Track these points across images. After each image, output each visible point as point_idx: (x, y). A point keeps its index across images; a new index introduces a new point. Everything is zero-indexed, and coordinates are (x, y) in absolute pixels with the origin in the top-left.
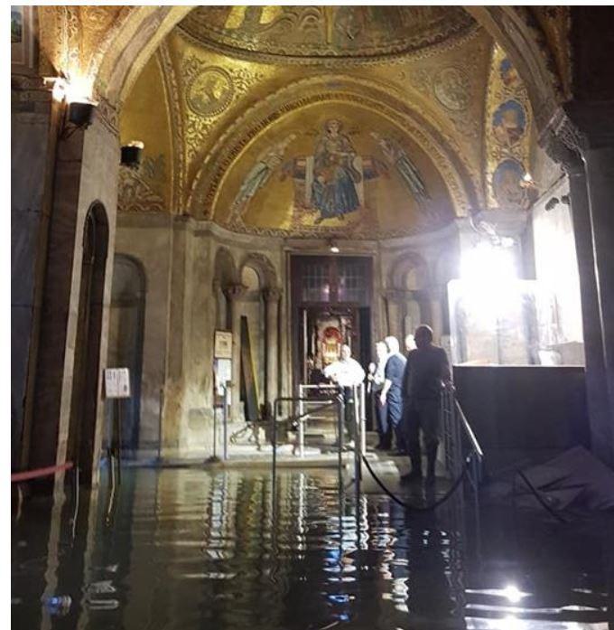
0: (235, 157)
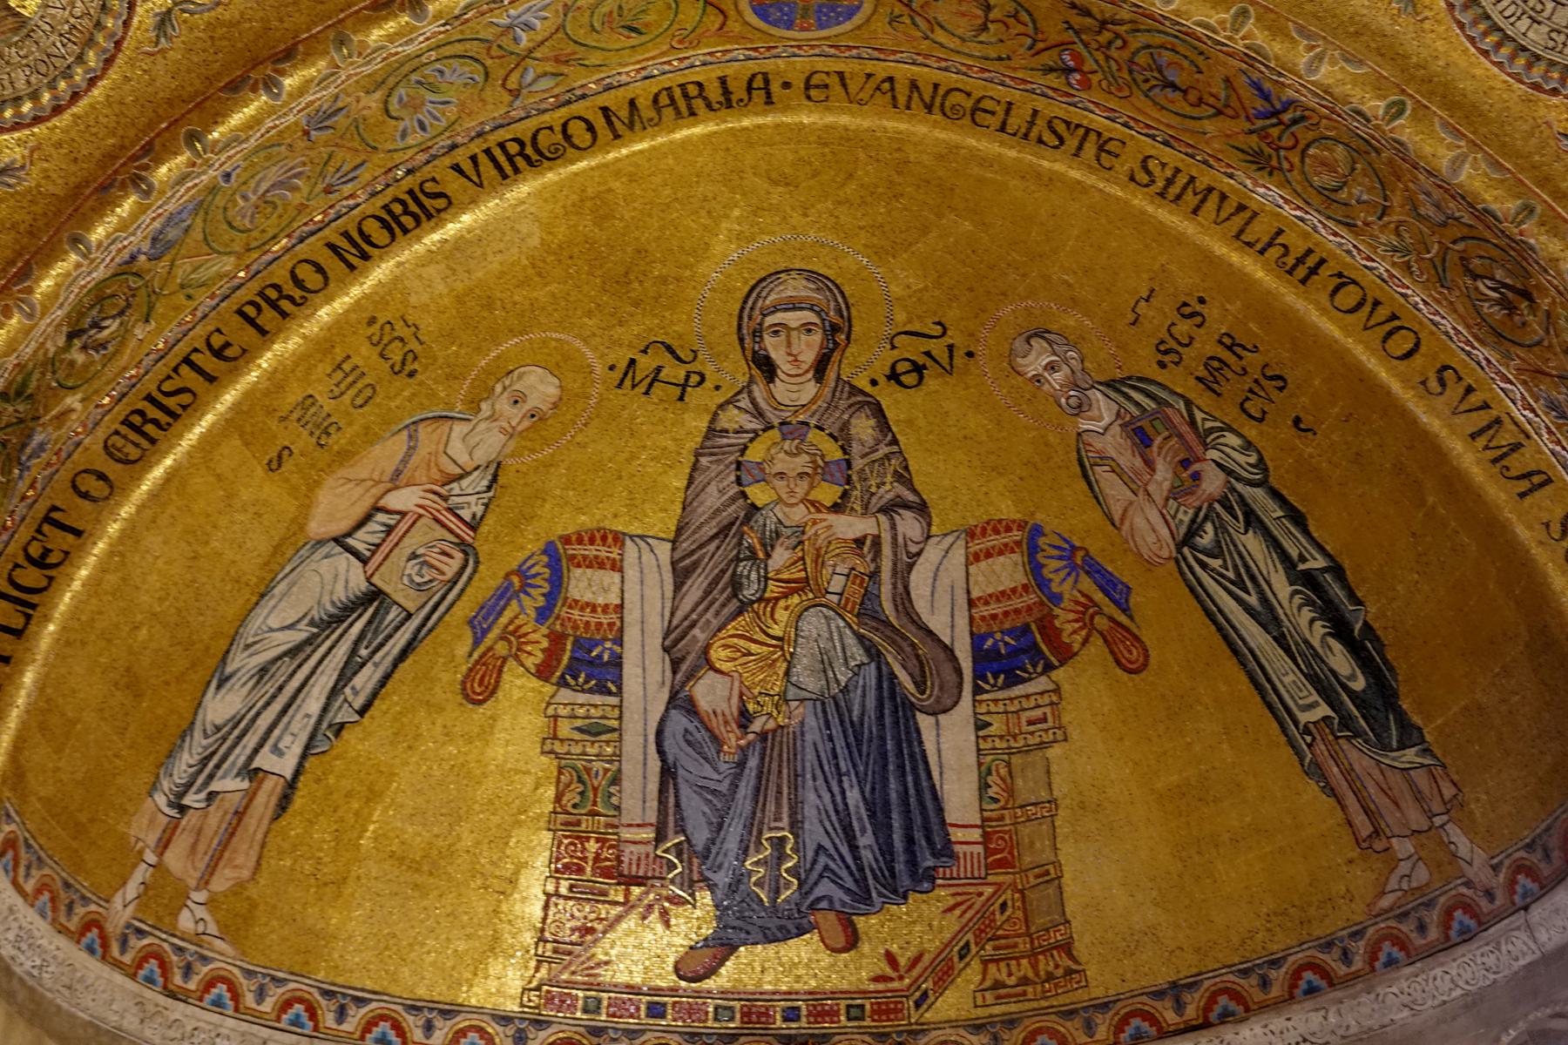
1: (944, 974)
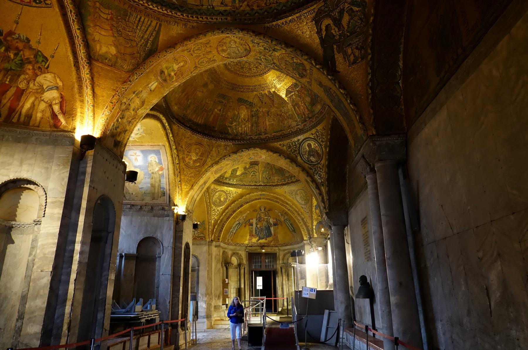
0: (228, 220)
1: (271, 242)
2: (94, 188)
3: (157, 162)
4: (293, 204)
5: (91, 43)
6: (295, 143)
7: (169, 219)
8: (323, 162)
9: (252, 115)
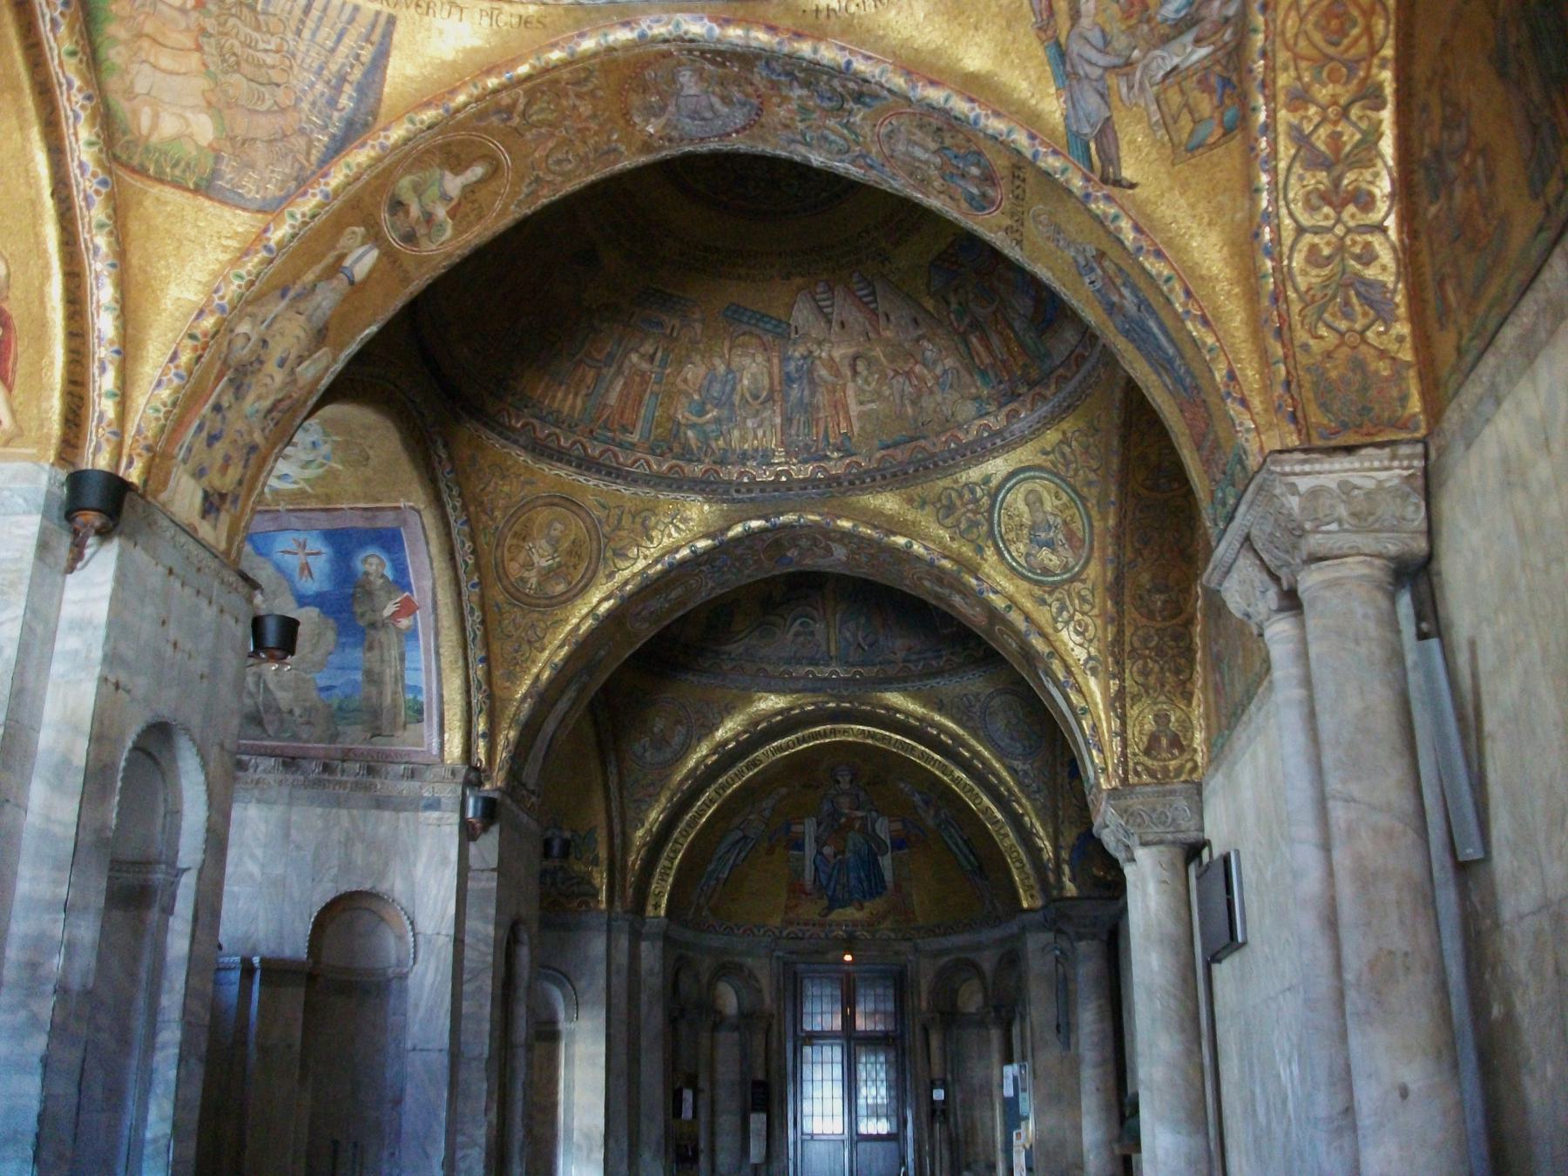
1: (884, 917)
2: (117, 686)
3: (391, 578)
4: (976, 754)
5: (120, 105)
6: (972, 492)
7: (440, 819)
8: (1093, 570)
9: (788, 374)
